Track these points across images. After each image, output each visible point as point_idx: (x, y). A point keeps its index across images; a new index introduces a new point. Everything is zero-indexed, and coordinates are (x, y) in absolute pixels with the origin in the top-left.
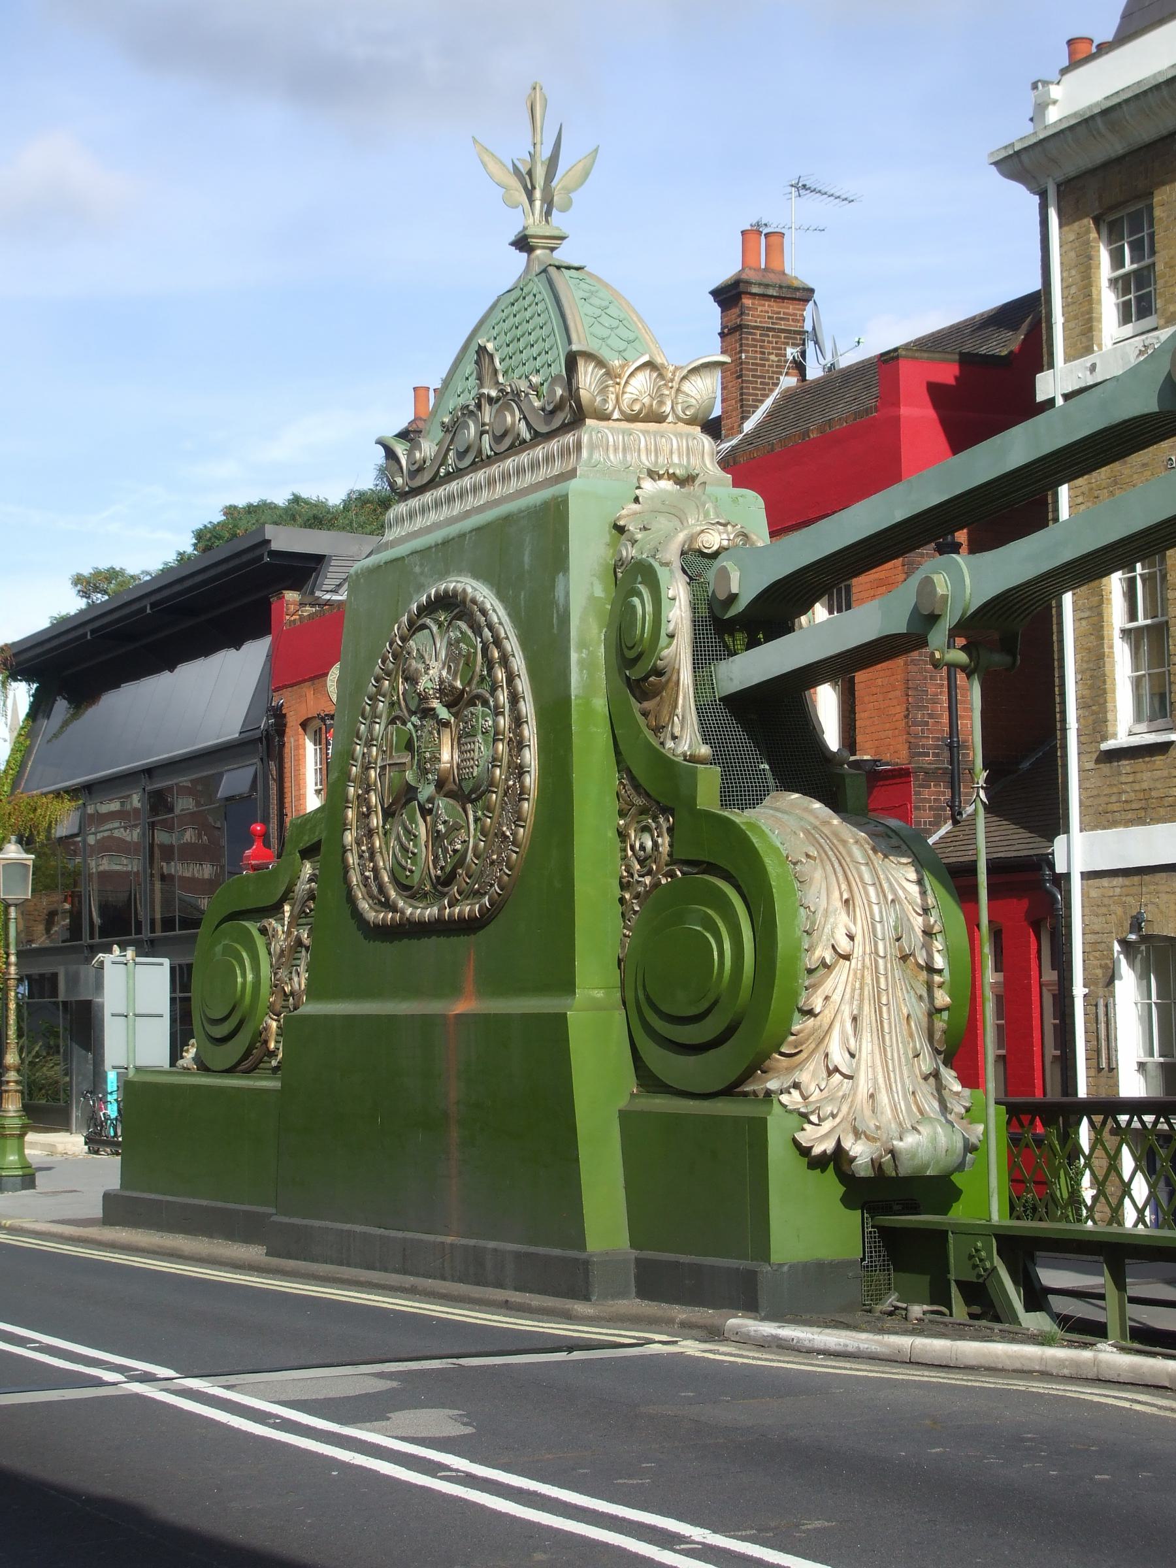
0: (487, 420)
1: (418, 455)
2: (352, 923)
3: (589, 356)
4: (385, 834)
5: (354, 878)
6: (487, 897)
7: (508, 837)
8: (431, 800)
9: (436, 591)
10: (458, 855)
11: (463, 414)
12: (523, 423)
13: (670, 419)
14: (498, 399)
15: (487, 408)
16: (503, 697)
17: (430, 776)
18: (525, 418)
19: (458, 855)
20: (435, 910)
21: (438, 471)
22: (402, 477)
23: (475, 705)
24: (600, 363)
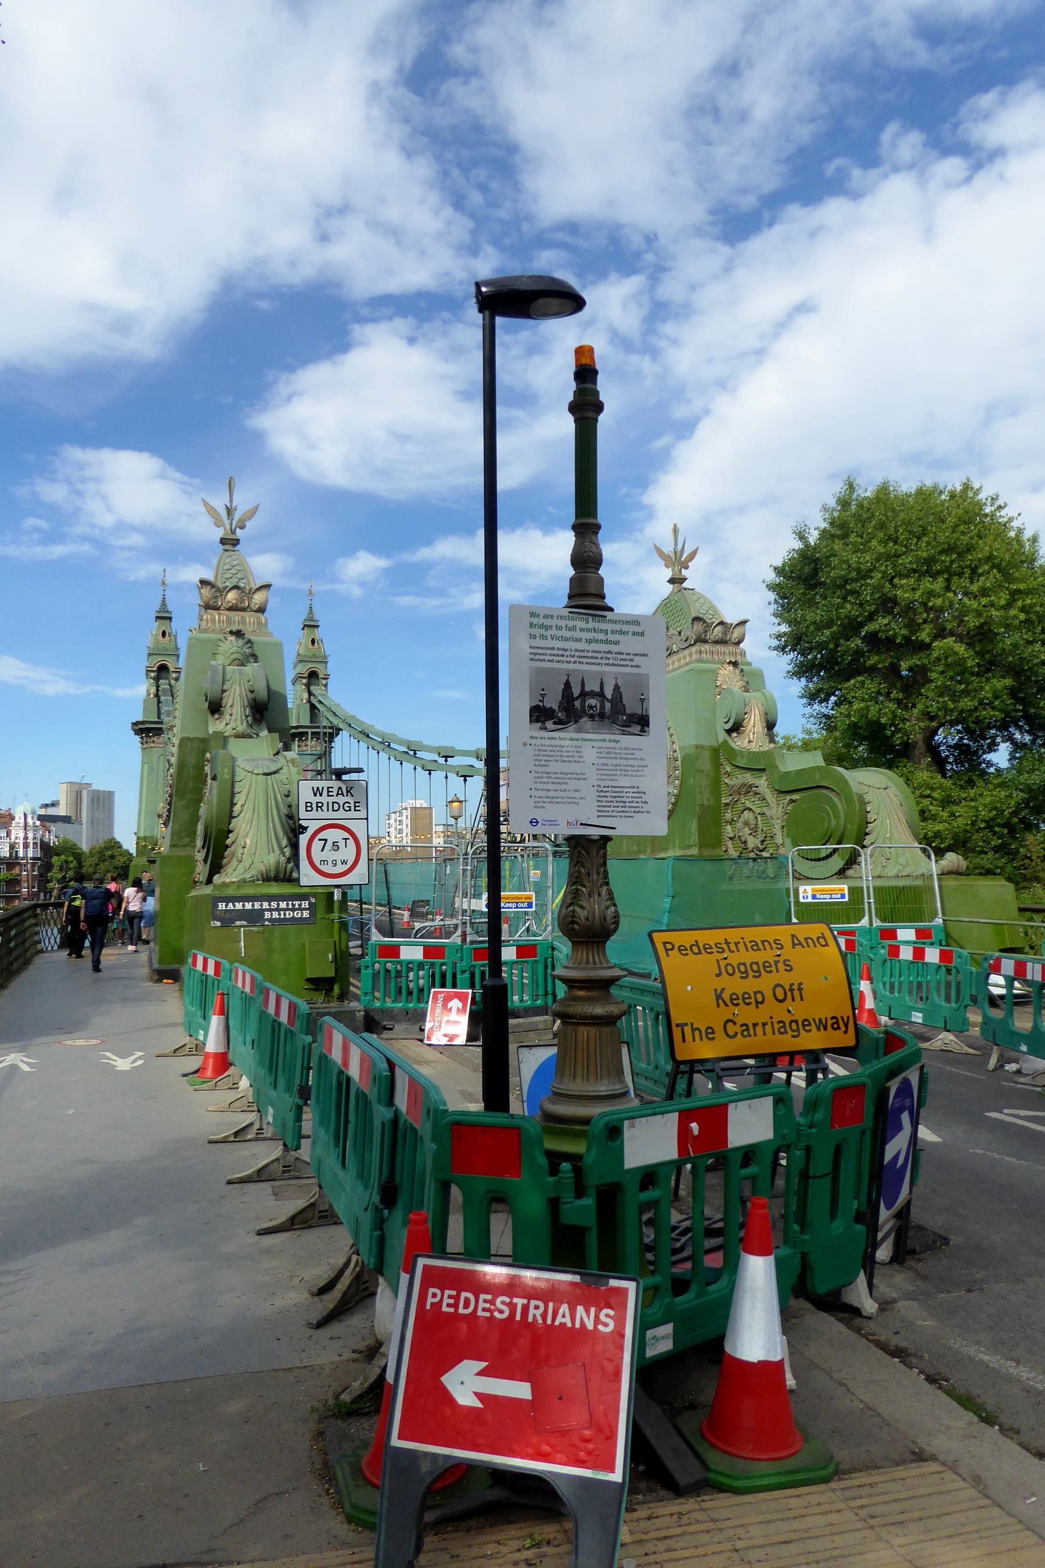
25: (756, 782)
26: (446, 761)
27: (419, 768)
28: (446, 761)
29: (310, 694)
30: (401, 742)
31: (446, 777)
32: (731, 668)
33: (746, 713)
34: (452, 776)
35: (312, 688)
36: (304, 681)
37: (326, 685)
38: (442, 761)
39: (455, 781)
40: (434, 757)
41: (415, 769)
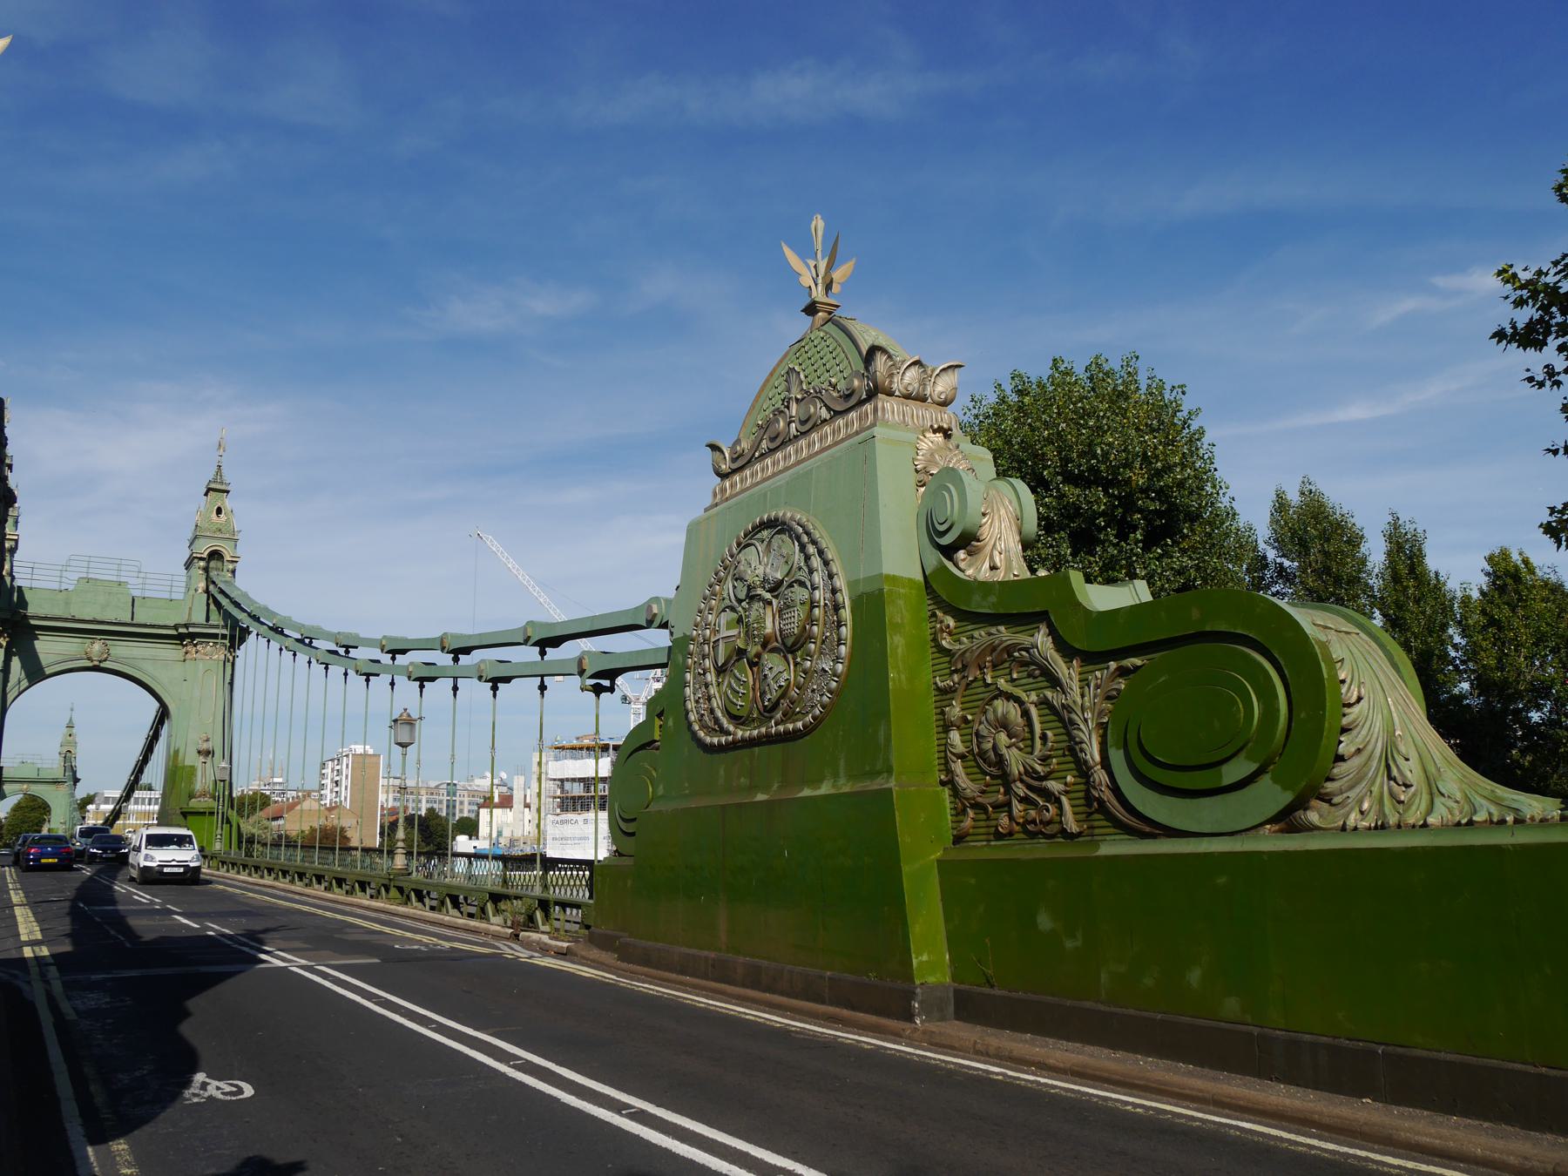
0: (794, 415)
1: (738, 448)
2: (694, 745)
3: (884, 351)
4: (718, 685)
5: (692, 717)
6: (810, 715)
7: (827, 671)
8: (758, 655)
9: (769, 516)
10: (783, 689)
11: (775, 415)
12: (824, 408)
13: (929, 400)
14: (803, 399)
15: (794, 407)
16: (817, 578)
17: (757, 640)
18: (826, 405)
19: (783, 689)
20: (763, 730)
21: (754, 454)
22: (726, 464)
23: (793, 586)
24: (890, 357)
25: (1024, 639)
26: (393, 659)
27: (351, 673)
28: (393, 659)
29: (209, 581)
30: (328, 636)
31: (392, 684)
32: (939, 437)
33: (984, 515)
34: (401, 680)
35: (213, 574)
36: (202, 564)
37: (233, 572)
38: (386, 659)
39: (407, 688)
40: (376, 654)
41: (346, 674)
